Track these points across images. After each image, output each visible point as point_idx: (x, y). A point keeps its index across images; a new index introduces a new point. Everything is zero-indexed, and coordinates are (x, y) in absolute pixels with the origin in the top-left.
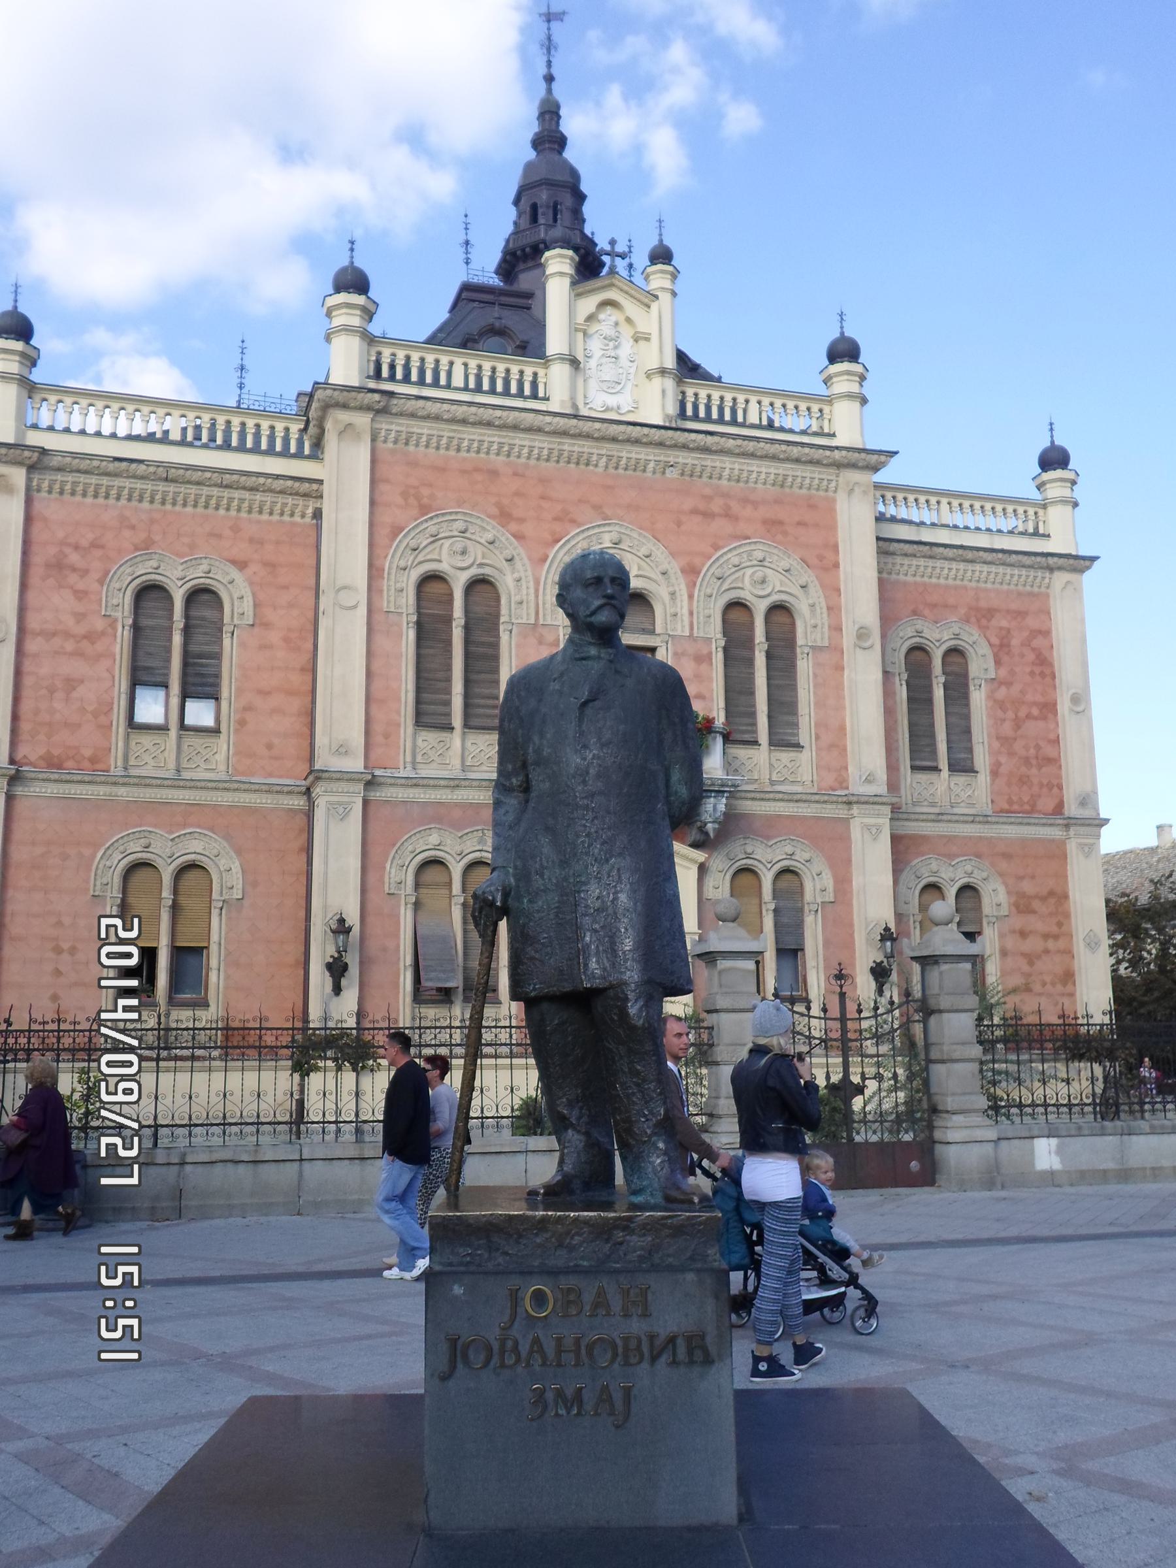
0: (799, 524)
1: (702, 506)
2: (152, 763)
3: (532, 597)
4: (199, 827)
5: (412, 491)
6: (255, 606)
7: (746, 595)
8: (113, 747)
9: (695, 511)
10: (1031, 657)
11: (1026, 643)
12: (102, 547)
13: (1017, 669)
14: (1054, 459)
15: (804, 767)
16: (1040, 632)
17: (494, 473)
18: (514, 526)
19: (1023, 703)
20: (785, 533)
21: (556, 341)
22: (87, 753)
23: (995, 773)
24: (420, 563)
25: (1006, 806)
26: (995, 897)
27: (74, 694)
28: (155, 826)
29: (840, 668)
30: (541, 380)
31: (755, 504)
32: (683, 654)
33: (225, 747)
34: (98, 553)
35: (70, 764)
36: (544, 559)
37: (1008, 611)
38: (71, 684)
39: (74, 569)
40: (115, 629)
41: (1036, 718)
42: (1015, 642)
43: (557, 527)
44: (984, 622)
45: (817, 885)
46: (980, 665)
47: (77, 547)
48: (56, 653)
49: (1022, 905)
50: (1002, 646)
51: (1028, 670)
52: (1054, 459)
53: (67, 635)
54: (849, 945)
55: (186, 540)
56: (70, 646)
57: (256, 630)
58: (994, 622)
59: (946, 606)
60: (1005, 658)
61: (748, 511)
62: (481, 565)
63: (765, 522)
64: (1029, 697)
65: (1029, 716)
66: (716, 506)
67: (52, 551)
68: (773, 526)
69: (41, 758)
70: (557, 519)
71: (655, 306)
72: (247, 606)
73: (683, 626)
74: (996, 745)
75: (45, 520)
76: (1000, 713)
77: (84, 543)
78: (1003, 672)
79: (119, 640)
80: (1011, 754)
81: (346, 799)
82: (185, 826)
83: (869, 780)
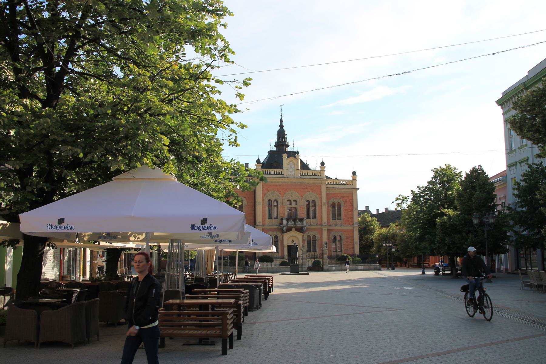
14: (354, 173)
15: (317, 220)
21: (284, 167)
26: (343, 237)
29: (321, 208)
45: (318, 237)
49: (347, 238)
52: (354, 173)
68: (313, 189)
72: (246, 203)
83: (325, 223)
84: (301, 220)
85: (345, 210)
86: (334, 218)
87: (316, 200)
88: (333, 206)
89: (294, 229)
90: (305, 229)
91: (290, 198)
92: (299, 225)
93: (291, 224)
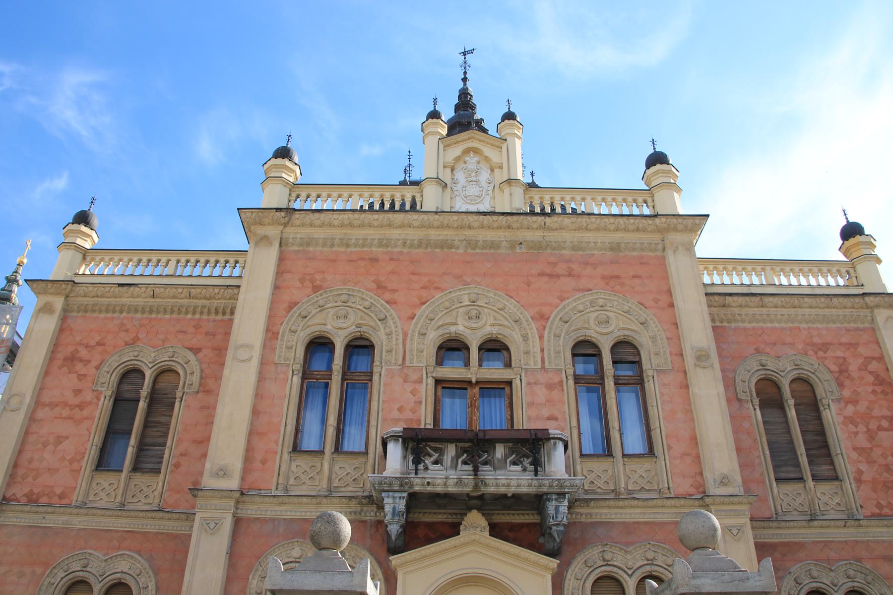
0: (634, 277)
1: (548, 271)
2: (106, 498)
3: (401, 346)
4: (129, 550)
5: (308, 277)
6: (201, 378)
7: (593, 333)
8: (79, 486)
9: (541, 274)
10: (871, 379)
11: (863, 367)
12: (104, 345)
13: (858, 390)
16: (873, 358)
17: (374, 260)
18: (388, 296)
19: (872, 417)
20: (622, 285)
22: (58, 491)
23: (859, 481)
24: (308, 327)
25: (877, 511)
27: (61, 447)
28: (96, 549)
30: (418, 200)
31: (595, 266)
32: (535, 383)
33: (160, 484)
34: (100, 348)
35: (44, 500)
36: (412, 317)
37: (841, 344)
38: (60, 439)
39: (81, 361)
40: (99, 399)
41: (887, 430)
42: (851, 368)
43: (424, 294)
44: (820, 354)
46: (826, 388)
47: (87, 346)
48: (56, 418)
50: (841, 372)
51: (870, 389)
53: (65, 404)
55: (161, 337)
56: (65, 412)
57: (200, 395)
58: (829, 353)
59: (784, 344)
60: (847, 382)
61: (589, 270)
62: (358, 326)
63: (603, 278)
64: (876, 412)
65: (880, 428)
66: (561, 269)
67: (71, 349)
68: (611, 280)
69: (25, 495)
70: (423, 288)
71: (504, 147)
72: (196, 379)
73: (535, 362)
74: (854, 455)
75: (71, 330)
76: (852, 428)
77: (93, 343)
78: (846, 393)
79: (100, 407)
80: (871, 462)
81: (217, 515)
82: (119, 549)
84: (531, 446)
85: (850, 420)
86: (785, 467)
87: (643, 340)
88: (769, 395)
89: (475, 521)
90: (558, 511)
91: (461, 328)
92: (508, 477)
93: (445, 475)
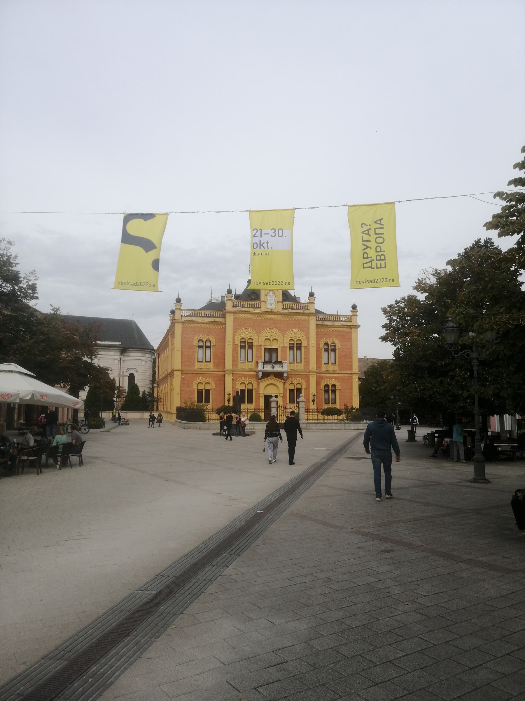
14: (354, 307)
21: (262, 298)
52: (354, 307)
54: (309, 395)
